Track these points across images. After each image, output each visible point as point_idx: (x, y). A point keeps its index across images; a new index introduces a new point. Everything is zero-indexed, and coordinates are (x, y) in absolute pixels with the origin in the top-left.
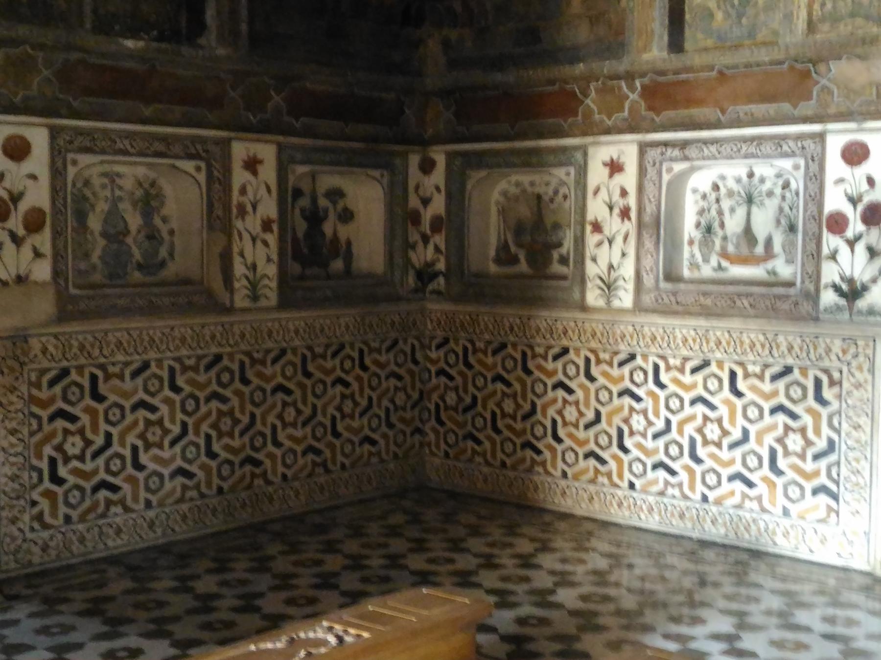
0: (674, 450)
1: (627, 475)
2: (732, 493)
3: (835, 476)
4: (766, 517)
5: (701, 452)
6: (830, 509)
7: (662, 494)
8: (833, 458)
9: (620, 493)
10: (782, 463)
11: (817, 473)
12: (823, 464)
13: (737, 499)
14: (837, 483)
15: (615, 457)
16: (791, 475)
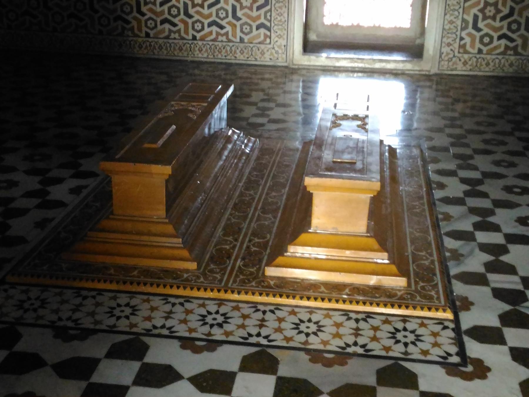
0: (174, 11)
1: (144, 29)
2: (211, 33)
3: (269, 17)
4: (231, 44)
5: (191, 11)
6: (266, 36)
7: (167, 37)
8: (268, 7)
9: (140, 40)
10: (239, 14)
11: (259, 17)
12: (262, 11)
13: (214, 36)
14: (270, 21)
15: (135, 18)
16: (244, 19)
